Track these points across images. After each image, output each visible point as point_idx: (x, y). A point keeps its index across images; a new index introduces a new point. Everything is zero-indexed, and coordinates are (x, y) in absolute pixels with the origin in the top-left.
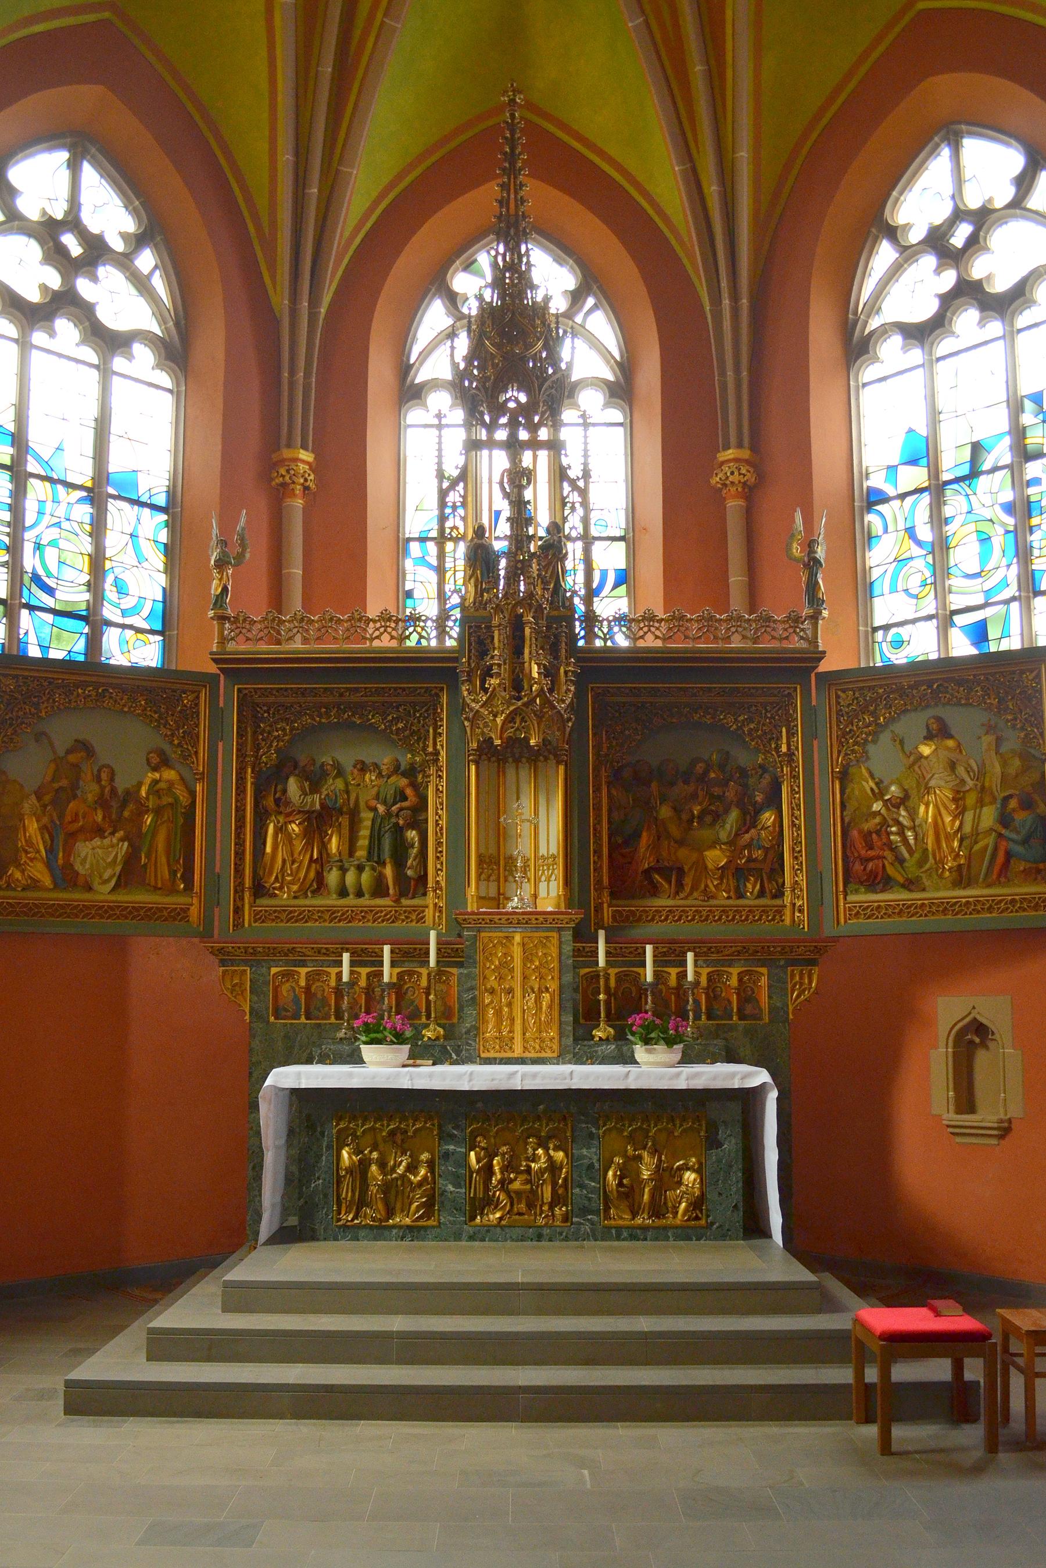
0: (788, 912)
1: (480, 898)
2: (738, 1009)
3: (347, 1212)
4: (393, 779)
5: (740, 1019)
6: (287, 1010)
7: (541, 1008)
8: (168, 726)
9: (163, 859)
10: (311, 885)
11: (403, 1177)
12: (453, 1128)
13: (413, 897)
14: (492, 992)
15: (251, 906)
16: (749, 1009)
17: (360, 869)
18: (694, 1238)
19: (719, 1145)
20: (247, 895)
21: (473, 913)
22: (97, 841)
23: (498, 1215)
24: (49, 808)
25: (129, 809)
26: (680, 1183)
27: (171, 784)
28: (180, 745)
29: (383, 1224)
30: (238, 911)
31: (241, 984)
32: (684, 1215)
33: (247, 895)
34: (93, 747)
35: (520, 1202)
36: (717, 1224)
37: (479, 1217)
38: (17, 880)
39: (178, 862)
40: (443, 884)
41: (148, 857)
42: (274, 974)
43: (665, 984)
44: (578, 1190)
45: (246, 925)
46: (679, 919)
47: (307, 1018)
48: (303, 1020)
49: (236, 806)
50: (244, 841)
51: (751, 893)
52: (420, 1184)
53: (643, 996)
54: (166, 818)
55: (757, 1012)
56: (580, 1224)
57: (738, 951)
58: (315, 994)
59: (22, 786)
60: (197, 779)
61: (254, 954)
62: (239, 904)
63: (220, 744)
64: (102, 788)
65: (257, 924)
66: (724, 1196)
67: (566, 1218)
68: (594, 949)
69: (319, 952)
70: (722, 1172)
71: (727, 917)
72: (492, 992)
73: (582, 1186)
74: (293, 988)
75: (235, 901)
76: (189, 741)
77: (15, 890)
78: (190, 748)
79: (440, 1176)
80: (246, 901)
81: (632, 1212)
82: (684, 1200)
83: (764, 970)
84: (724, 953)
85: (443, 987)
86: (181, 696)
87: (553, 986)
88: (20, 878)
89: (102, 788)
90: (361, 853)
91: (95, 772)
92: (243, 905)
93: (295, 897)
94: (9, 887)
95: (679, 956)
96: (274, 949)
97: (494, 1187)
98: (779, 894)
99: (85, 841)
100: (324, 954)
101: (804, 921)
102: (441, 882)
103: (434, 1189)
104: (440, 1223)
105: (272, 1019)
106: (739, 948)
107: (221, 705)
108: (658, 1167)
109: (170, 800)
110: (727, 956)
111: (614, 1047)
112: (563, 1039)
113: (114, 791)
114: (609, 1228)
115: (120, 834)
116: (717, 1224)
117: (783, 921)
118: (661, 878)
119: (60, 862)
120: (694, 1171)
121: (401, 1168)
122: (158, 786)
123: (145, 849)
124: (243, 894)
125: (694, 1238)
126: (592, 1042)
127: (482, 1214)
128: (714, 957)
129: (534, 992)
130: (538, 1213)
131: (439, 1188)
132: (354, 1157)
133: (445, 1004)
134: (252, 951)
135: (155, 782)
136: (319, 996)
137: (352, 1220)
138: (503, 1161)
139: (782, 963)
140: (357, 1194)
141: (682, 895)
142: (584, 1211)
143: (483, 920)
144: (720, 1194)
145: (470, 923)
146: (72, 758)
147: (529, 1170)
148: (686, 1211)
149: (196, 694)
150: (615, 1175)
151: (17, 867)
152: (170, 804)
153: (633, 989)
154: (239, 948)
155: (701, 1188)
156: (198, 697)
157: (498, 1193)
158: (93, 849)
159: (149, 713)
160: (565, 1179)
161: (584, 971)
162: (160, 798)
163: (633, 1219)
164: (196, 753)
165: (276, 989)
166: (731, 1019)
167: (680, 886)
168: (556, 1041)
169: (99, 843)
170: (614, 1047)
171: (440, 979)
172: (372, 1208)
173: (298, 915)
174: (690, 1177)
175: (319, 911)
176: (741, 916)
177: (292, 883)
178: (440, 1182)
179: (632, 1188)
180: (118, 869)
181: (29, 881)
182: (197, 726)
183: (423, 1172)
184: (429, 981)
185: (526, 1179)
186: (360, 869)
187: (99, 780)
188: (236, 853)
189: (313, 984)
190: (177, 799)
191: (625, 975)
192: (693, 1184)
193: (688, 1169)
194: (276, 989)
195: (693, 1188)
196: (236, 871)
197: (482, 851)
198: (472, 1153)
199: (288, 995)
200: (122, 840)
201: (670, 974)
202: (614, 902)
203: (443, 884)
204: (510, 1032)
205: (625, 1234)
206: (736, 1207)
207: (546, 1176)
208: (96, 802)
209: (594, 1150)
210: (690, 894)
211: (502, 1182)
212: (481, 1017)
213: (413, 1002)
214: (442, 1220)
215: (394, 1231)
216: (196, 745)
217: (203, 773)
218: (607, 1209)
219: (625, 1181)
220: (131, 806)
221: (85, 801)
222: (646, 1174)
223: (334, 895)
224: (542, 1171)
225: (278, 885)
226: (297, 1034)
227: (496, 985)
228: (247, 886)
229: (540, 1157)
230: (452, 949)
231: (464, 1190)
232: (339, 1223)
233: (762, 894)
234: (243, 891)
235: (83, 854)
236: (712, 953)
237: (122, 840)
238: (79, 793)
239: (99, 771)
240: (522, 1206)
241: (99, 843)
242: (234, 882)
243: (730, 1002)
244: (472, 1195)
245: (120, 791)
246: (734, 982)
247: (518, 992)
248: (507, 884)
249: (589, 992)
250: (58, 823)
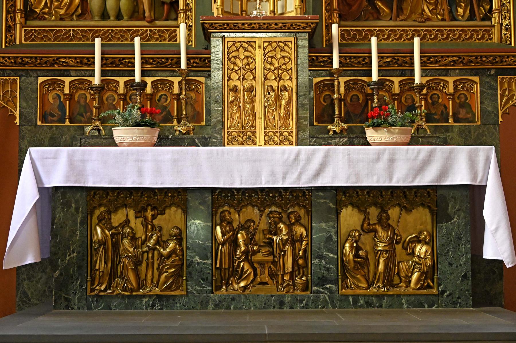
0: (496, 31)
2: (453, 113)
3: (100, 284)
5: (455, 121)
6: (53, 116)
7: (280, 105)
10: (76, 10)
11: (153, 249)
12: (200, 203)
13: (167, 20)
14: (235, 89)
15: (22, 26)
16: (462, 114)
18: (426, 306)
19: (449, 219)
20: (19, 15)
21: (218, 18)
23: (242, 284)
26: (412, 254)
29: (134, 293)
30: (10, 29)
31: (13, 92)
32: (417, 283)
33: (19, 15)
35: (262, 273)
36: (448, 293)
37: (224, 287)
40: (193, 7)
42: (41, 84)
43: (389, 91)
44: (317, 260)
45: (18, 42)
46: (400, 38)
47: (71, 122)
48: (67, 123)
51: (462, 16)
52: (169, 255)
53: (370, 102)
55: (470, 116)
56: (318, 292)
57: (454, 61)
58: (78, 101)
61: (23, 64)
62: (11, 23)
65: (28, 43)
66: (454, 266)
67: (306, 288)
68: (326, 59)
69: (81, 62)
70: (452, 244)
71: (442, 35)
73: (321, 257)
74: (59, 96)
75: (7, 20)
79: (187, 248)
80: (18, 21)
81: (367, 281)
82: (416, 270)
83: (477, 79)
84: (442, 63)
85: (193, 95)
87: (291, 84)
92: (15, 25)
93: (62, 19)
95: (401, 66)
96: (41, 58)
97: (239, 258)
98: (487, 17)
100: (86, 64)
101: (511, 38)
102: (191, 4)
103: (182, 260)
104: (187, 292)
105: (39, 123)
106: (455, 58)
108: (392, 239)
110: (443, 66)
111: (346, 139)
112: (300, 133)
114: (347, 296)
116: (448, 293)
117: (491, 39)
118: (383, 4)
120: (426, 243)
121: (152, 241)
124: (15, 16)
125: (426, 306)
126: (327, 136)
127: (227, 284)
128: (433, 66)
129: (274, 91)
130: (280, 283)
131: (187, 260)
132: (107, 232)
133: (194, 110)
134: (20, 61)
136: (82, 101)
137: (105, 290)
138: (247, 235)
139: (493, 72)
140: (109, 265)
141: (401, 18)
142: (323, 281)
143: (228, 24)
144: (450, 264)
145: (216, 28)
147: (270, 243)
148: (419, 280)
150: (351, 247)
153: (361, 97)
154: (9, 58)
155: (432, 259)
157: (242, 264)
160: (305, 251)
161: (317, 80)
163: (369, 288)
165: (44, 97)
166: (448, 122)
167: (400, 10)
168: (294, 135)
170: (346, 139)
171: (189, 87)
172: (123, 279)
173: (64, 35)
174: (421, 249)
175: (82, 31)
176: (454, 35)
177: (59, 7)
178: (188, 253)
179: (367, 259)
183: (172, 245)
184: (180, 89)
185: (269, 251)
189: (76, 92)
191: (353, 84)
192: (425, 255)
193: (419, 242)
194: (44, 97)
195: (425, 258)
198: (218, 228)
199: (54, 102)
201: (393, 82)
202: (343, 23)
203: (193, 7)
204: (252, 126)
205: (362, 302)
206: (465, 277)
207: (287, 247)
209: (332, 223)
210: (409, 16)
211: (245, 253)
213: (165, 107)
214: (190, 289)
215: (145, 300)
218: (345, 278)
219: (361, 253)
222: (381, 247)
223: (97, 18)
224: (284, 243)
225: (47, 10)
226: (62, 136)
227: (238, 84)
228: (19, 8)
229: (282, 230)
230: (201, 58)
231: (210, 262)
232: (93, 294)
233: (472, 17)
234: (14, 12)
236: (431, 63)
240: (266, 277)
242: (7, 4)
243: (446, 108)
244: (218, 266)
246: (451, 89)
247: (260, 91)
248: (249, 3)
249: (322, 100)
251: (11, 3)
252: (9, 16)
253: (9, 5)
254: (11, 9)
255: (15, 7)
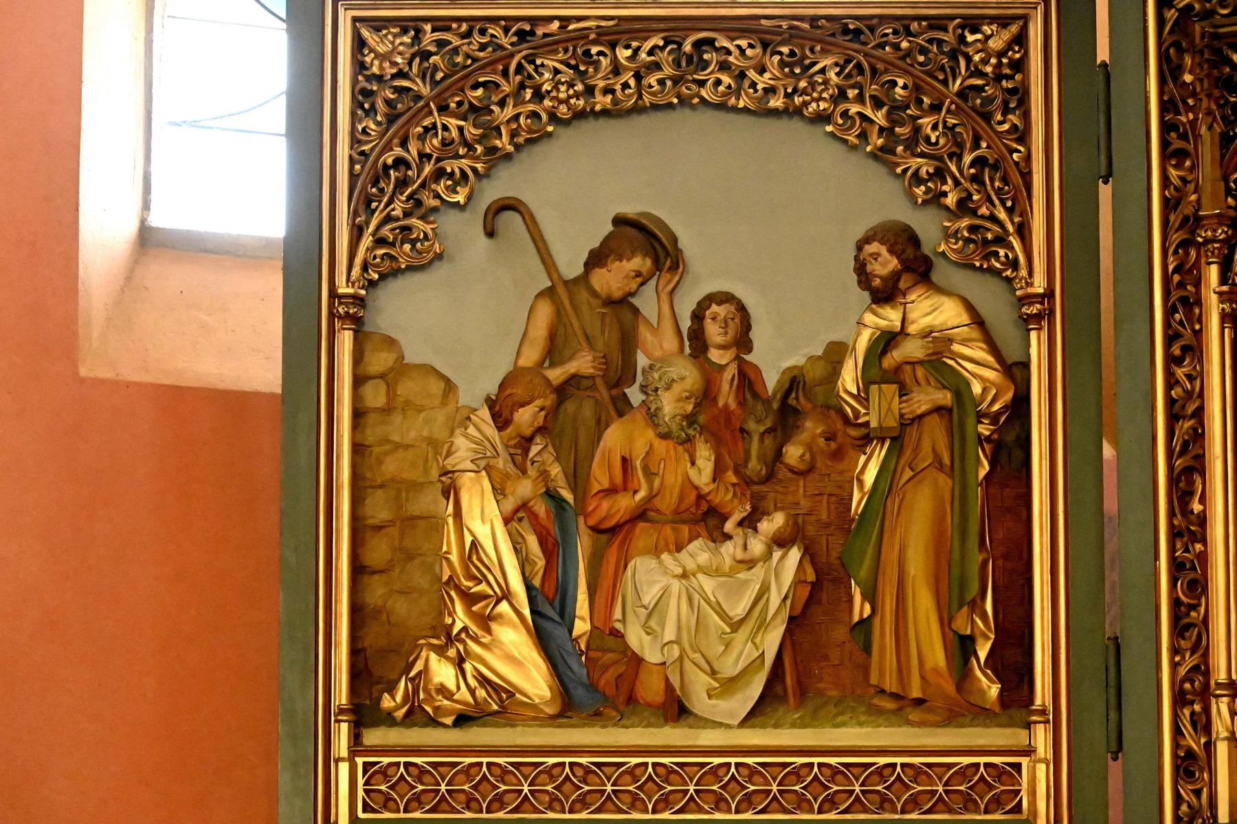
8: (922, 147)
9: (923, 604)
22: (699, 552)
24: (534, 450)
25: (804, 436)
27: (940, 342)
28: (964, 206)
34: (675, 240)
38: (442, 690)
39: (976, 605)
41: (871, 595)
49: (1170, 402)
50: (1202, 520)
54: (926, 459)
59: (449, 386)
60: (1027, 320)
63: (1105, 192)
64: (710, 373)
75: (1177, 732)
76: (999, 192)
77: (434, 722)
78: (1002, 215)
86: (962, 39)
88: (451, 685)
89: (710, 373)
91: (686, 324)
92: (1209, 747)
94: (415, 715)
99: (656, 552)
107: (1103, 54)
109: (945, 398)
113: (747, 379)
115: (773, 523)
119: (581, 627)
122: (897, 355)
123: (864, 571)
124: (1207, 710)
135: (888, 340)
146: (610, 279)
149: (1014, 29)
151: (441, 651)
152: (939, 409)
156: (1021, 39)
158: (684, 575)
159: (854, 109)
162: (903, 392)
164: (1023, 231)
169: (704, 558)
180: (772, 640)
181: (481, 693)
182: (1022, 135)
187: (698, 342)
188: (1177, 567)
190: (959, 388)
196: (1179, 628)
200: (781, 542)
208: (690, 419)
216: (1019, 207)
217: (1049, 294)
220: (812, 428)
221: (652, 416)
234: (1205, 694)
235: (649, 597)
237: (781, 542)
238: (635, 395)
239: (698, 317)
241: (704, 558)
242: (1174, 666)
245: (771, 381)
250: (568, 495)
251: (1190, 661)
252: (1187, 712)
253: (1182, 671)
254: (1192, 682)
255: (1207, 674)
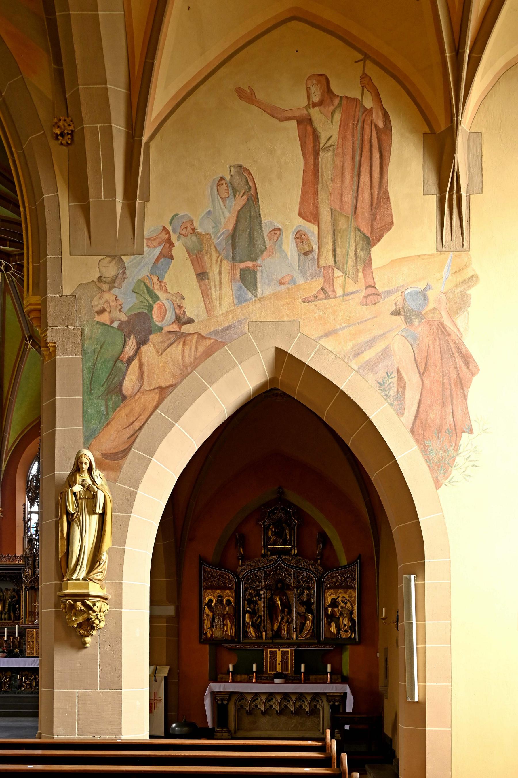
1: (29, 621)
4: (13, 593)
14: (29, 642)
17: (5, 614)
72: (29, 642)
90: (6, 610)
186: (5, 614)
197: (30, 610)
212: (26, 648)
227: (30, 640)
247: (35, 642)
